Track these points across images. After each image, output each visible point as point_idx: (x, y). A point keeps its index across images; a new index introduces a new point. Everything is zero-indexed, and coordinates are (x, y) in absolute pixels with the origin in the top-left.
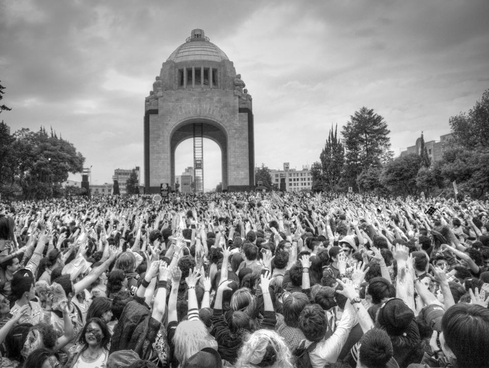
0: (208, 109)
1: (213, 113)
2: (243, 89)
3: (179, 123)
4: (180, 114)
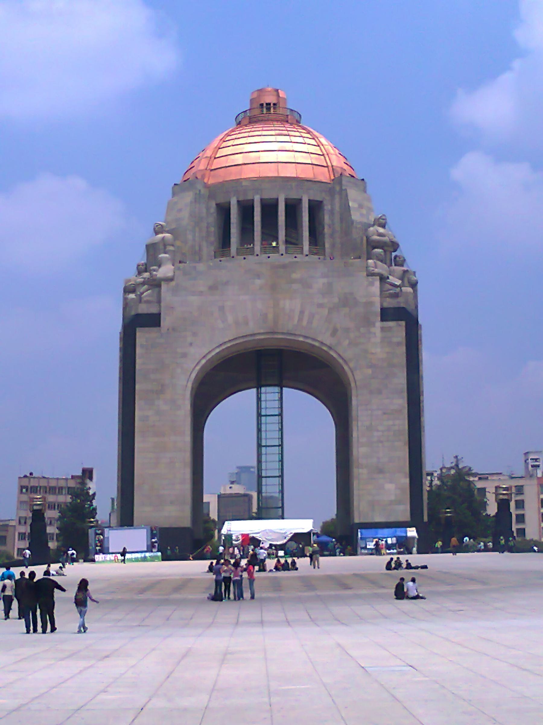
0: (297, 313)
1: (310, 322)
2: (394, 254)
3: (218, 350)
4: (221, 325)
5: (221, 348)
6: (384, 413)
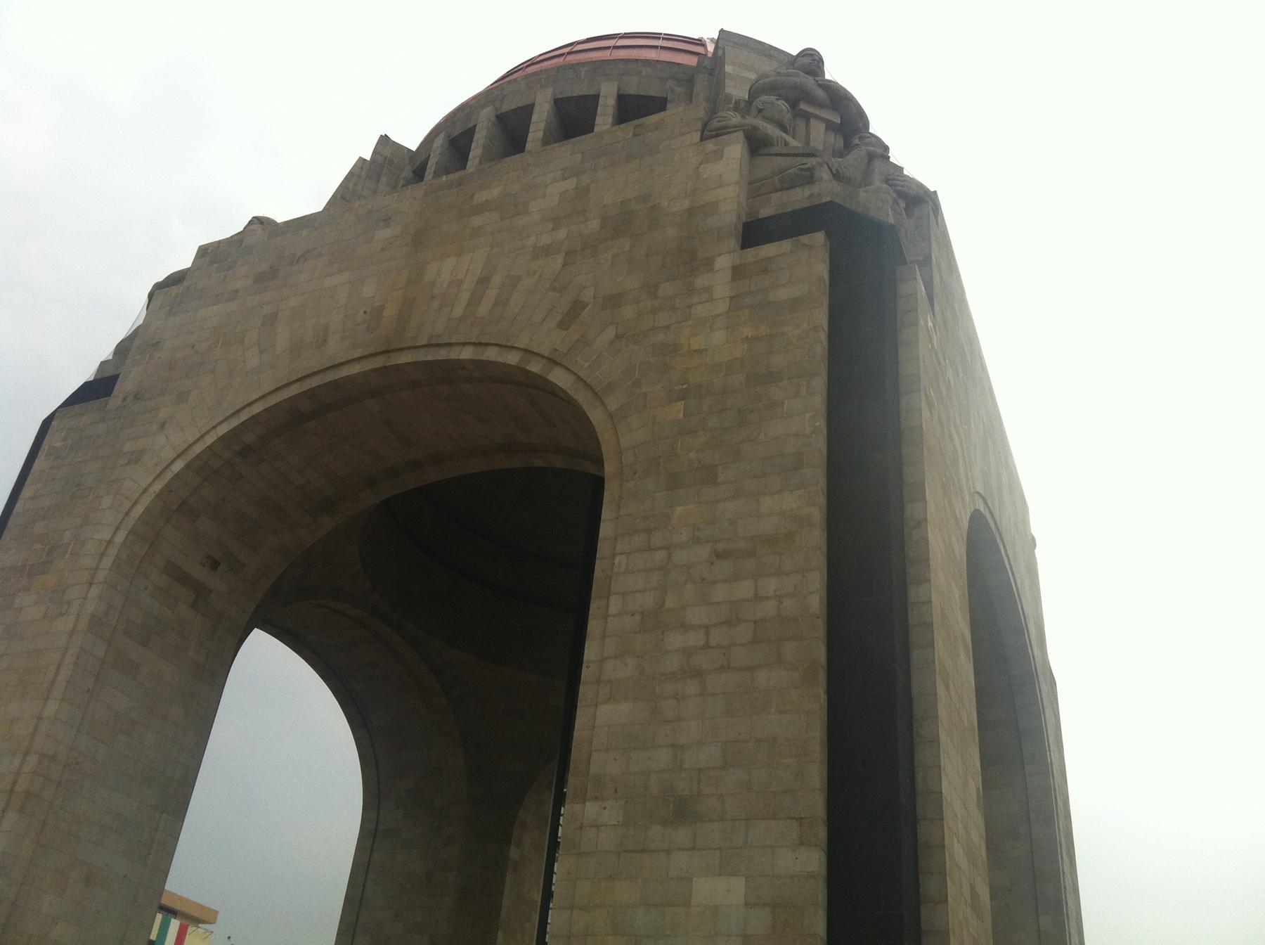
3: (224, 429)
5: (235, 423)
6: (720, 555)
